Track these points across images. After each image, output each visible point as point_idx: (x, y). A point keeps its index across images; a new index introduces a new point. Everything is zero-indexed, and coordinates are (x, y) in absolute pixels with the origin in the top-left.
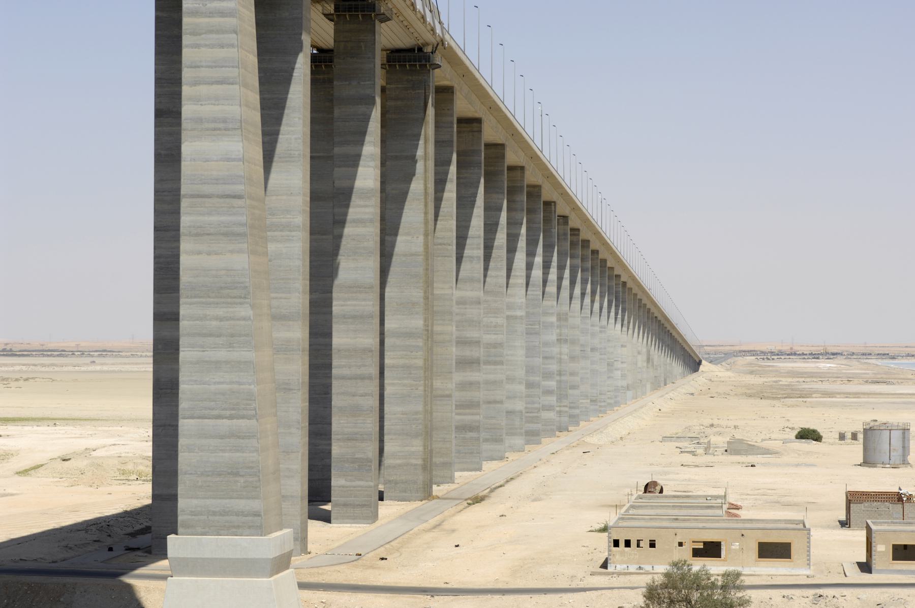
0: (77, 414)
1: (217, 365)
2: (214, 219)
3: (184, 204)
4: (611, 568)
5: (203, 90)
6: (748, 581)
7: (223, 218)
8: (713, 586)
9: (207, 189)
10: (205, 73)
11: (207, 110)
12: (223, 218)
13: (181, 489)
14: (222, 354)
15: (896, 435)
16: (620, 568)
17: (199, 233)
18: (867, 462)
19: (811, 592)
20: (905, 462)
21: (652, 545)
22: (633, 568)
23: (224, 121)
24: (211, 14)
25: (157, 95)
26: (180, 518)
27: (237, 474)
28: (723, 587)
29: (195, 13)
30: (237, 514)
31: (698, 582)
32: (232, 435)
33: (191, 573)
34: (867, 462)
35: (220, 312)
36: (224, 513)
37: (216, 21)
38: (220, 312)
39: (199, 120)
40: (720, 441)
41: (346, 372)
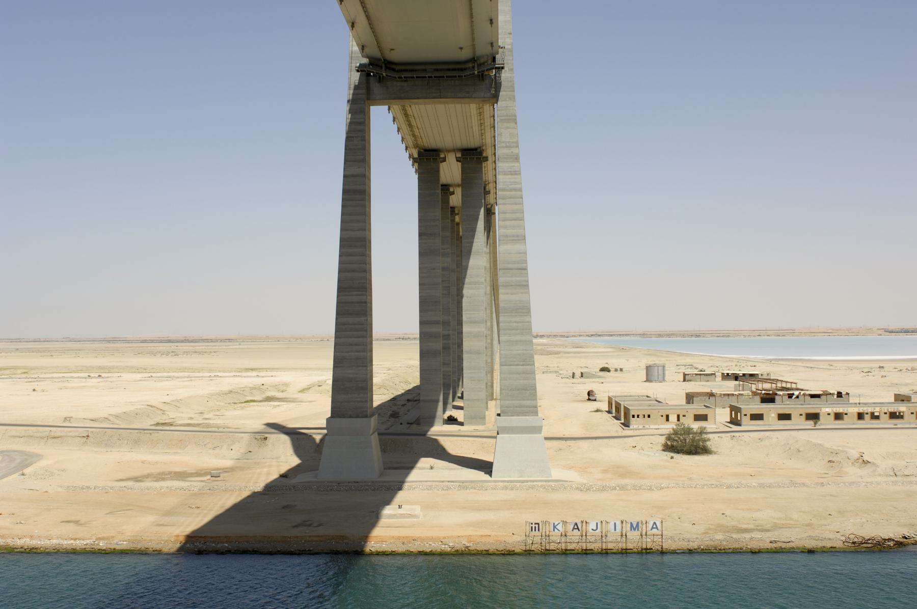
0: (264, 366)
1: (516, 342)
2: (514, 279)
4: (631, 427)
6: (709, 430)
7: (518, 279)
8: (696, 433)
9: (510, 266)
12: (518, 279)
14: (518, 338)
15: (660, 368)
16: (635, 427)
17: (507, 285)
18: (648, 380)
19: (729, 435)
20: (664, 380)
21: (649, 416)
22: (641, 427)
23: (518, 236)
24: (511, 190)
25: (420, 227)
27: (526, 390)
28: (701, 433)
29: (503, 190)
30: (527, 407)
31: (689, 431)
33: (508, 433)
34: (648, 380)
35: (518, 319)
36: (521, 406)
37: (513, 193)
38: (518, 319)
40: (578, 374)
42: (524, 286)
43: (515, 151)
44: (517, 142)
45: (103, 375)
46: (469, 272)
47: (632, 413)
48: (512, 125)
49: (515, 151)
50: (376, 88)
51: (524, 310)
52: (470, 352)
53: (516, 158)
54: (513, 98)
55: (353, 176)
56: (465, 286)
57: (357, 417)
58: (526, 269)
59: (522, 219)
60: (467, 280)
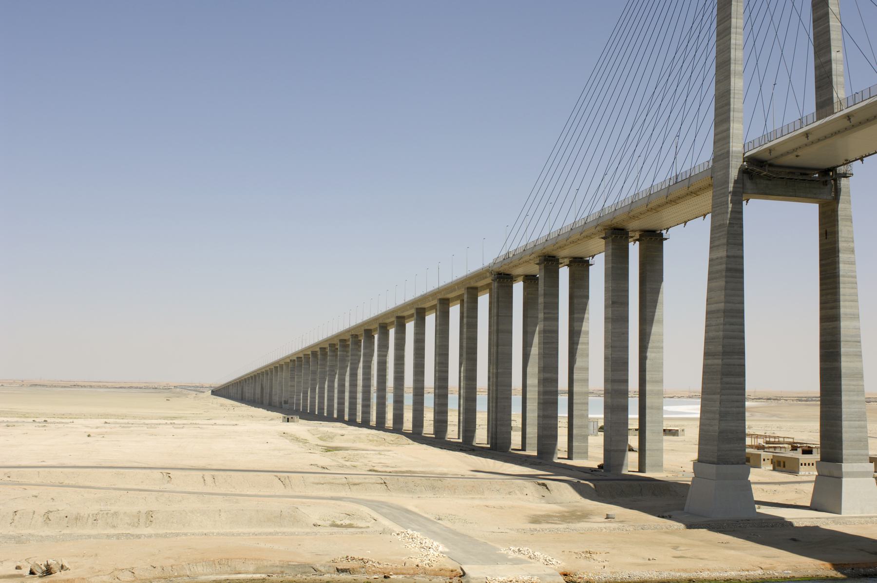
1: (854, 402)
2: (852, 350)
3: (842, 344)
5: (847, 304)
10: (847, 298)
11: (848, 311)
13: (844, 446)
14: (855, 398)
16: (803, 473)
24: (849, 277)
26: (844, 457)
29: (844, 276)
32: (860, 427)
35: (854, 383)
36: (858, 455)
37: (850, 279)
38: (854, 383)
39: (846, 314)
41: (578, 401)
42: (859, 355)
43: (851, 245)
44: (852, 238)
45: (49, 420)
46: (652, 338)
47: (801, 462)
48: (849, 223)
49: (851, 245)
50: (749, 184)
51: (859, 375)
52: (652, 408)
53: (852, 251)
54: (849, 202)
55: (734, 257)
56: (649, 350)
57: (738, 464)
58: (859, 342)
59: (857, 301)
60: (650, 345)
